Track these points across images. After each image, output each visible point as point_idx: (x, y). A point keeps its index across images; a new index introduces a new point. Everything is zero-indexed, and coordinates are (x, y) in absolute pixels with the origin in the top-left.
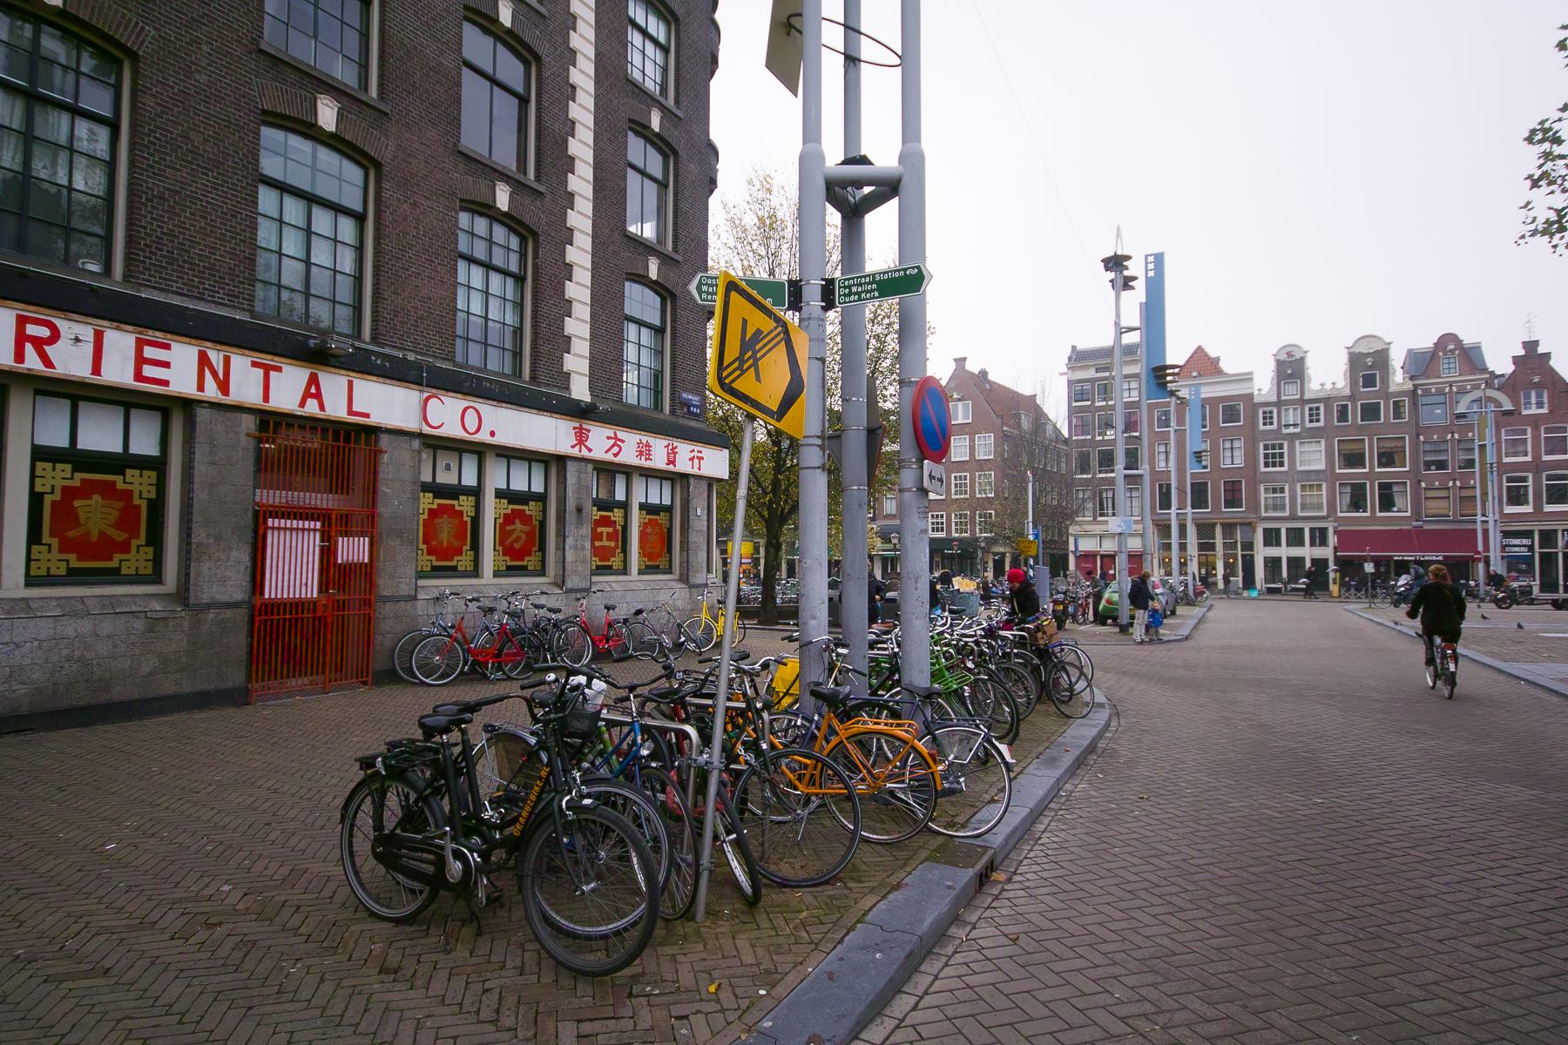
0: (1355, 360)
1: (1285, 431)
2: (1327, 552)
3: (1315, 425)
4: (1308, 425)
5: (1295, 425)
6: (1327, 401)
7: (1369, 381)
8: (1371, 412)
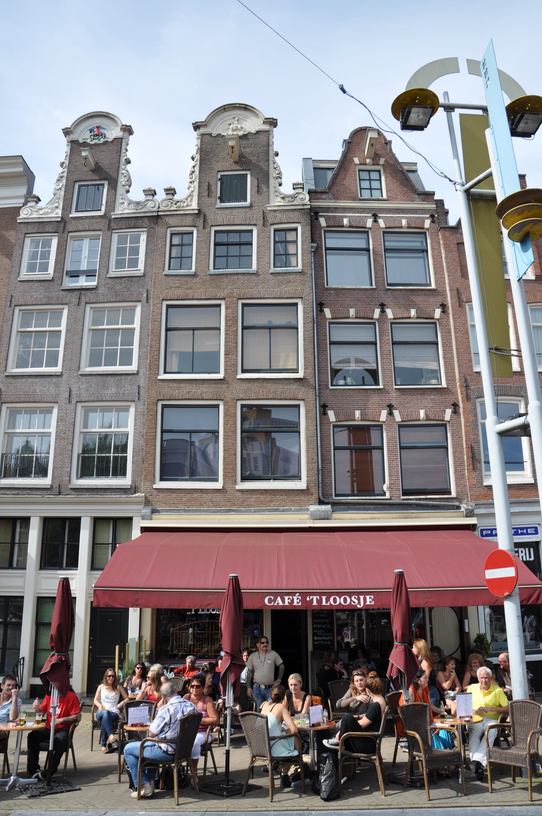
0: (209, 149)
1: (69, 283)
3: (127, 271)
4: (113, 272)
5: (90, 274)
8: (232, 245)
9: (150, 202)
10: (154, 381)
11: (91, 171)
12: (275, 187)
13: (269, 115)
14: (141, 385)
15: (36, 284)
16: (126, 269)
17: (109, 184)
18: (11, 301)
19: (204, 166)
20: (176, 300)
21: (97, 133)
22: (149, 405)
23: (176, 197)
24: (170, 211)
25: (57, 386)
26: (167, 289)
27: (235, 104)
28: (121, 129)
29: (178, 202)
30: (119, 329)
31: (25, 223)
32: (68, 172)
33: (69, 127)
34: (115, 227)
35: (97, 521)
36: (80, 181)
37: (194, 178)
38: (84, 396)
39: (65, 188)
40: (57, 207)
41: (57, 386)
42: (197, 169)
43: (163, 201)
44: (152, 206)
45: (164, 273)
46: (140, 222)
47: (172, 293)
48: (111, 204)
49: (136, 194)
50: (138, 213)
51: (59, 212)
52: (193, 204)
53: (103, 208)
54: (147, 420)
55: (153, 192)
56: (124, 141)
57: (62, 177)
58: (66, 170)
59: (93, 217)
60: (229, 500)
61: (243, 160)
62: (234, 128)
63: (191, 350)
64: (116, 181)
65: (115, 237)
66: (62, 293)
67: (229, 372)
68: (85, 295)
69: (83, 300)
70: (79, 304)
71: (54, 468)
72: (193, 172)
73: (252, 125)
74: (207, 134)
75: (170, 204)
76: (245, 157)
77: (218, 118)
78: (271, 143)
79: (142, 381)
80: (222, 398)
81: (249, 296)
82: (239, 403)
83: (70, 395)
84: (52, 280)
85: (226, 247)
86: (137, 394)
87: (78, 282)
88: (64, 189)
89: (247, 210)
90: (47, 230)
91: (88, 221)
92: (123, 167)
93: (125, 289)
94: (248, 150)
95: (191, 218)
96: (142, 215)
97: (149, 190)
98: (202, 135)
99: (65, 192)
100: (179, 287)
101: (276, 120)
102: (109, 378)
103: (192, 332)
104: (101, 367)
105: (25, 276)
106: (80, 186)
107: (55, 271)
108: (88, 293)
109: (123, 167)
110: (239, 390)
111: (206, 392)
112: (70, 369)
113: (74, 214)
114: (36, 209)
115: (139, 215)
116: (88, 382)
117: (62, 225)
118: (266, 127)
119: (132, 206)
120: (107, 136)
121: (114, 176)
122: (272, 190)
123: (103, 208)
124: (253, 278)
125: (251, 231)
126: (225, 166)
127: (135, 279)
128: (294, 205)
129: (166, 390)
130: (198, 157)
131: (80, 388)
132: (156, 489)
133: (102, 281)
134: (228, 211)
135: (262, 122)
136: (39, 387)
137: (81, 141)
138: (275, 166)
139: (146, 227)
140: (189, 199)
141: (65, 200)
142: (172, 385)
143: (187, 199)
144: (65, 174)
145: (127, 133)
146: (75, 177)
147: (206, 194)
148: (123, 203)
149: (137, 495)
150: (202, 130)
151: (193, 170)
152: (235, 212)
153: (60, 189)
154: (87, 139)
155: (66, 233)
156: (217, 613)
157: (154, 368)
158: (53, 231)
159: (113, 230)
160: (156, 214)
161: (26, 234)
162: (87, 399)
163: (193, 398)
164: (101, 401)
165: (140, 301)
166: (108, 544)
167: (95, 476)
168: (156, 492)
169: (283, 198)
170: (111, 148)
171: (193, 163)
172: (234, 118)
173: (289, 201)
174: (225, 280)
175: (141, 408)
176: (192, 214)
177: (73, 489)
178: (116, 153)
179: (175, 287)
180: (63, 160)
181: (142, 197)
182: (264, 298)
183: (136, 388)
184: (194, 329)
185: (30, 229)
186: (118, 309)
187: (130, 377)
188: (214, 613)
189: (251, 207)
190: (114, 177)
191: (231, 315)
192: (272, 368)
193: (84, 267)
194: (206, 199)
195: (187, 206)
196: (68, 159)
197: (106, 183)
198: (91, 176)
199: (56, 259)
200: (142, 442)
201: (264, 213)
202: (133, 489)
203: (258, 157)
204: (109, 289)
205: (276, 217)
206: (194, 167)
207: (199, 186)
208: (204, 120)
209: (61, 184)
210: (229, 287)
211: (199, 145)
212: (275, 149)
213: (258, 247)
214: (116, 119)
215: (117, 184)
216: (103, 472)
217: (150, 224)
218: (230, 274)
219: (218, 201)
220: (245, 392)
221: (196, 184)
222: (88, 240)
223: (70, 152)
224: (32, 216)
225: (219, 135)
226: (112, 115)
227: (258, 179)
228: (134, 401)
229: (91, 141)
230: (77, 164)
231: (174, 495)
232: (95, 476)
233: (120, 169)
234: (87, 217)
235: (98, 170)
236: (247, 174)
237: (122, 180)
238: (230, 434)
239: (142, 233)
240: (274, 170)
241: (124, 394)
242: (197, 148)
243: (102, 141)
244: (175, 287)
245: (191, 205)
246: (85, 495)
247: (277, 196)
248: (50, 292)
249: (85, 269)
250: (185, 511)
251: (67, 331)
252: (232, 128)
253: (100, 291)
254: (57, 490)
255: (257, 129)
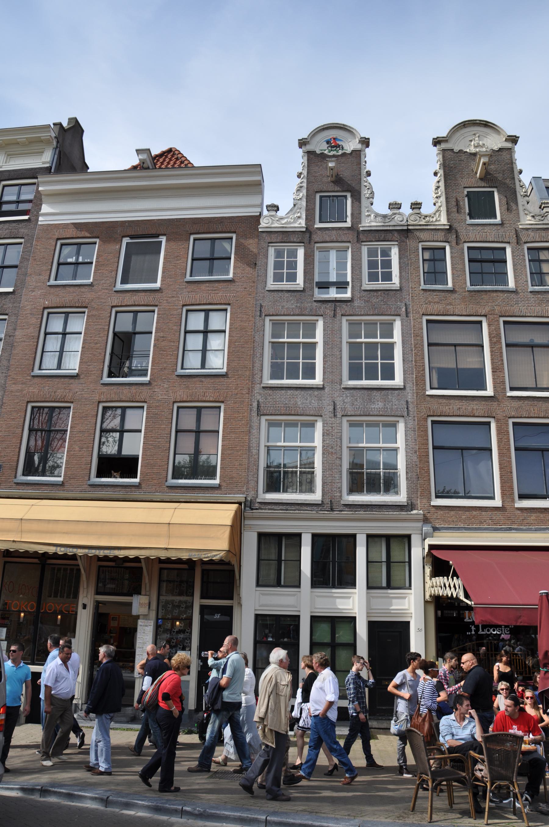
0: (452, 165)
1: (319, 295)
2: (410, 606)
3: (380, 285)
4: (367, 285)
5: (341, 285)
6: (404, 234)
7: (481, 206)
9: (397, 216)
10: (422, 397)
11: (333, 182)
12: (523, 205)
13: (511, 132)
14: (409, 400)
15: (287, 295)
16: (285, 283)
17: (352, 196)
18: (260, 311)
19: (449, 181)
20: (437, 315)
21: (333, 144)
22: (419, 421)
23: (424, 211)
24: (420, 225)
25: (320, 399)
26: (427, 304)
27: (476, 120)
28: (359, 141)
29: (426, 216)
30: (300, 343)
31: (267, 232)
32: (308, 183)
33: (306, 137)
34: (365, 240)
35: (370, 537)
36: (321, 192)
37: (440, 193)
38: (350, 410)
39: (306, 199)
40: (299, 217)
41: (320, 399)
42: (442, 184)
43: (411, 215)
44: (401, 219)
45: (421, 288)
46: (389, 236)
47: (431, 308)
48: (357, 216)
49: (381, 207)
50: (387, 226)
51: (302, 223)
52: (442, 219)
53: (349, 219)
54: (417, 436)
55: (276, 209)
56: (362, 153)
57: (301, 187)
58: (305, 181)
59: (340, 228)
60: (509, 518)
61: (488, 177)
62: (476, 145)
63: (455, 366)
64: (359, 193)
65: (365, 250)
66: (315, 304)
67: (499, 389)
68: (340, 306)
69: (338, 311)
70: (335, 316)
71: (324, 483)
72: (438, 187)
73: (494, 142)
74: (448, 150)
75: (418, 218)
76: (490, 174)
77: (458, 134)
78: (514, 161)
79: (410, 395)
80: (494, 415)
81: (511, 314)
82: (511, 421)
83: (334, 409)
84: (303, 291)
85: (479, 264)
86: (406, 410)
87: (329, 294)
88: (305, 200)
89: (499, 227)
90: (292, 240)
91: (334, 232)
92: (365, 179)
93: (384, 302)
94: (492, 167)
95: (443, 234)
96: (391, 228)
97: (396, 204)
98: (444, 150)
99: (307, 202)
100: (438, 303)
101: (519, 137)
102: (374, 393)
103: (453, 348)
104: (362, 381)
105: (273, 286)
106: (321, 197)
107: (305, 282)
108: (344, 305)
109: (365, 179)
110: (509, 408)
111: (477, 409)
112: (332, 382)
113: (318, 225)
114: (277, 219)
115: (388, 228)
116: (353, 396)
117: (307, 235)
118: (509, 145)
119: (379, 219)
120: (345, 148)
121: (357, 188)
122: (521, 208)
123: (349, 219)
124: (513, 295)
125: (504, 249)
126: (471, 182)
127: (392, 293)
128: (544, 224)
129: (435, 406)
130: (441, 172)
131: (345, 402)
132: (433, 506)
133: (357, 294)
134: (480, 228)
135: (504, 139)
136: (300, 400)
137: (318, 152)
138: (522, 184)
139: (397, 241)
140: (437, 214)
141: (307, 210)
142: (441, 401)
143: (435, 214)
144: (305, 185)
145: (365, 146)
146: (316, 187)
147: (455, 210)
148: (369, 216)
149: (415, 512)
150: (444, 146)
151: (437, 185)
152: (487, 229)
153: (300, 199)
154: (325, 150)
155: (312, 243)
156: (498, 633)
157: (420, 382)
158: (298, 240)
159: (362, 242)
160: (405, 228)
161: (269, 243)
162: (353, 413)
163: (464, 414)
164: (368, 415)
165: (400, 315)
166: (405, 562)
167: (365, 493)
168: (433, 509)
169: (533, 216)
170: (350, 160)
171: (437, 179)
172: (475, 134)
173: (540, 220)
174: (484, 296)
175: (411, 423)
176: (443, 229)
177: (346, 505)
178: (357, 165)
179: (435, 303)
180: (300, 170)
181: (386, 211)
182: (526, 316)
183: (404, 403)
184: (455, 345)
185: (274, 238)
186: (297, 323)
187: (396, 392)
188: (495, 633)
189: (502, 224)
190: (357, 189)
191: (494, 332)
192: (538, 386)
193: (333, 278)
194: (455, 215)
195: (436, 221)
196: (306, 169)
197: (349, 195)
198: (331, 187)
199: (304, 270)
200: (415, 458)
201: (516, 231)
202: (409, 506)
203: (504, 175)
204: (366, 301)
205: (528, 236)
206: (438, 182)
207: (446, 202)
208: (445, 135)
209: (301, 194)
210: (490, 304)
211: (441, 160)
212: (518, 168)
213: (514, 265)
214: (354, 131)
215: (360, 196)
216: (373, 488)
217: (401, 237)
218: (489, 291)
219: (468, 217)
220: (517, 409)
221: (443, 199)
222: (335, 251)
223: (308, 163)
224: (273, 226)
225: (460, 151)
226: (350, 127)
227: (506, 197)
228: (403, 416)
229: (329, 152)
230: (317, 175)
231: (452, 513)
232: (365, 493)
233: (362, 181)
234: (333, 229)
235: (338, 181)
236: (493, 192)
237: (365, 193)
238: (505, 451)
239: (392, 247)
240: (521, 188)
241: (392, 409)
242: (439, 163)
243: (340, 152)
244: (435, 303)
245: (440, 220)
246: (359, 511)
247: (526, 214)
248: (302, 303)
249: (335, 280)
250: (466, 529)
251: (325, 343)
252: (474, 145)
253: (356, 303)
254: (329, 505)
255: (500, 146)
